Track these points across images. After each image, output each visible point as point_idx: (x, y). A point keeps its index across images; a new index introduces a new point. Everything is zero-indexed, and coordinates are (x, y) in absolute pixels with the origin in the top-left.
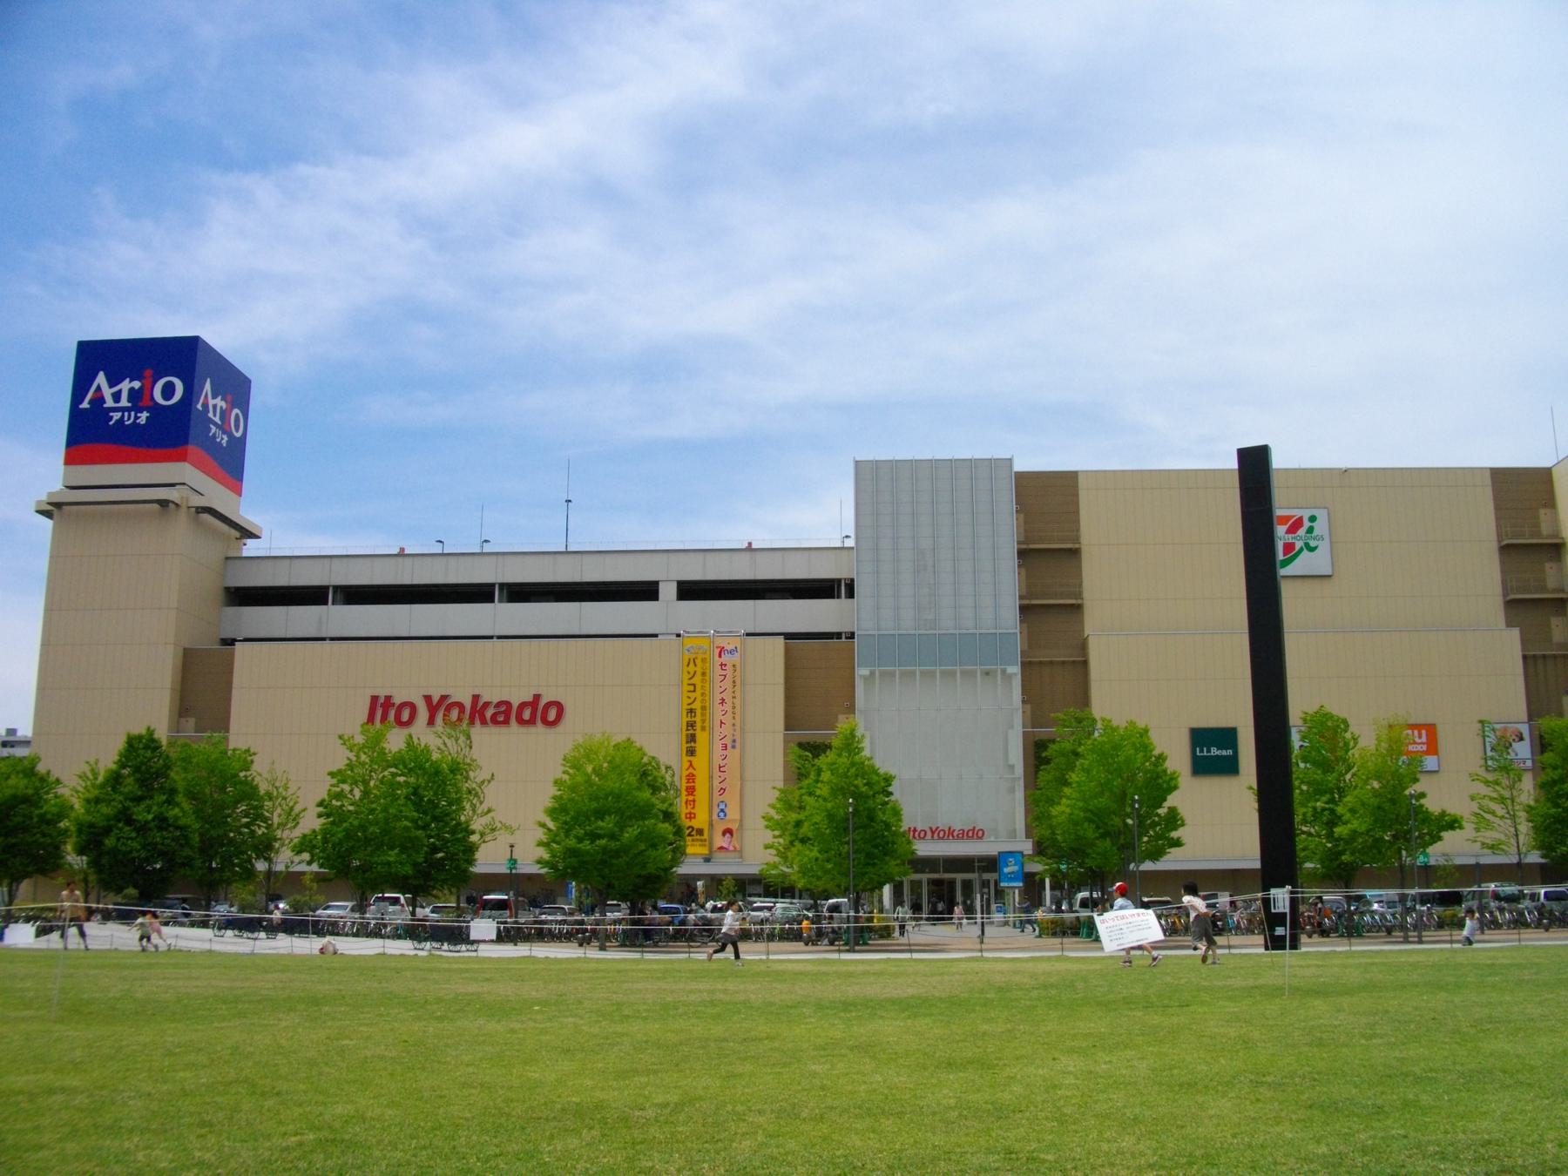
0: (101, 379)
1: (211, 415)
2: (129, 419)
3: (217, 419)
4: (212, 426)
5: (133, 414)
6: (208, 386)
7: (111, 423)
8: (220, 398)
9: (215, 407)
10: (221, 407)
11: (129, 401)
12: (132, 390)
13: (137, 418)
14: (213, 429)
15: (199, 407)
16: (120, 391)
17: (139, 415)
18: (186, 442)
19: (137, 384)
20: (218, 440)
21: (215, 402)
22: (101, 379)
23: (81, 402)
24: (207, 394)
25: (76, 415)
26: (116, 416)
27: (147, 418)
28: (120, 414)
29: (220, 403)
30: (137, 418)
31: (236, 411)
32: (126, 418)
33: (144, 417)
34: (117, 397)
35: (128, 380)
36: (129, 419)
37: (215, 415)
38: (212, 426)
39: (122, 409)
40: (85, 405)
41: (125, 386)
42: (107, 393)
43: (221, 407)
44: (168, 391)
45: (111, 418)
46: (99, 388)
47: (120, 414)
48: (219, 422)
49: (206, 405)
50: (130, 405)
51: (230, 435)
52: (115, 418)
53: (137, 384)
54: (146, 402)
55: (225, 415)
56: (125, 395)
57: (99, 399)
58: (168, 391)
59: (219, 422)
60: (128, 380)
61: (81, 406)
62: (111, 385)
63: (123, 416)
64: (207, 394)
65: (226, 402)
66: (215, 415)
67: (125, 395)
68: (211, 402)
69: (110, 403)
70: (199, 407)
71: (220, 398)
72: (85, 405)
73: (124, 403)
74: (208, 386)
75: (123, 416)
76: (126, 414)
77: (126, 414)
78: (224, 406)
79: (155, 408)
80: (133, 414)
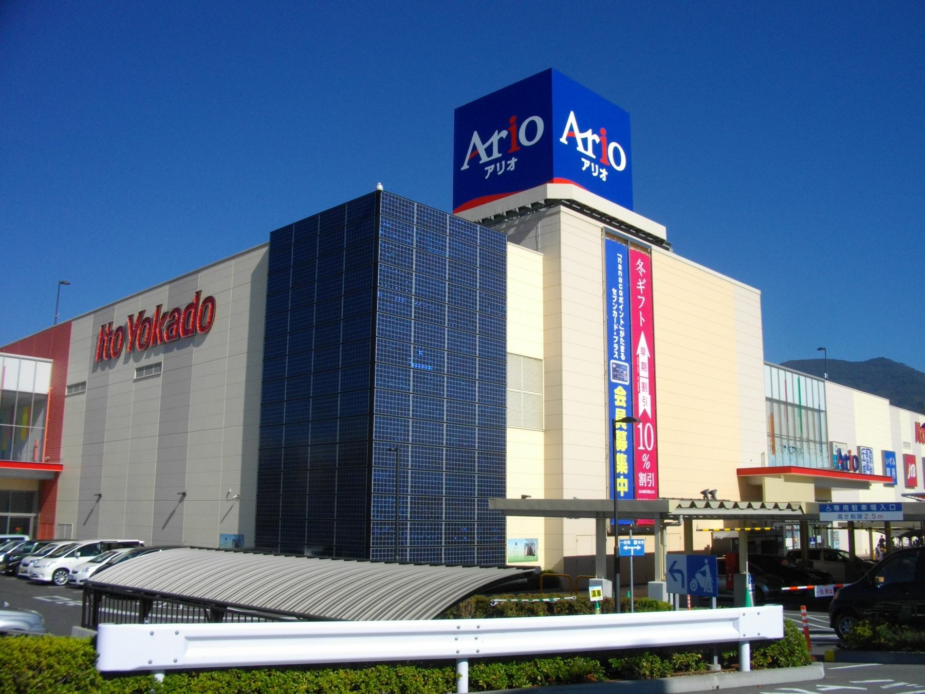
0: (476, 138)
1: (580, 148)
2: (501, 169)
3: (590, 153)
4: (583, 160)
5: (503, 163)
6: (572, 119)
7: (487, 177)
8: (590, 131)
9: (585, 141)
10: (594, 141)
11: (499, 152)
12: (501, 141)
13: (507, 166)
14: (587, 163)
15: (563, 140)
16: (492, 144)
17: (509, 162)
18: (553, 178)
19: (504, 134)
20: (595, 174)
21: (584, 135)
22: (476, 138)
23: (462, 165)
24: (571, 126)
25: (459, 176)
26: (490, 169)
27: (516, 163)
28: (493, 166)
29: (590, 135)
30: (507, 166)
31: (613, 145)
32: (498, 170)
34: (489, 151)
35: (497, 132)
36: (501, 169)
37: (586, 148)
38: (583, 160)
39: (494, 162)
40: (465, 166)
41: (495, 139)
42: (481, 149)
43: (594, 141)
46: (474, 146)
47: (493, 166)
48: (594, 157)
49: (572, 139)
50: (500, 155)
51: (610, 169)
52: (490, 171)
53: (504, 134)
55: (599, 149)
57: (476, 157)
59: (594, 157)
61: (462, 169)
63: (496, 167)
64: (571, 126)
65: (599, 135)
66: (586, 148)
68: (579, 136)
69: (484, 158)
70: (563, 140)
71: (590, 131)
73: (496, 154)
74: (572, 119)
75: (496, 167)
76: (498, 165)
77: (498, 165)
78: (598, 140)
80: (503, 163)
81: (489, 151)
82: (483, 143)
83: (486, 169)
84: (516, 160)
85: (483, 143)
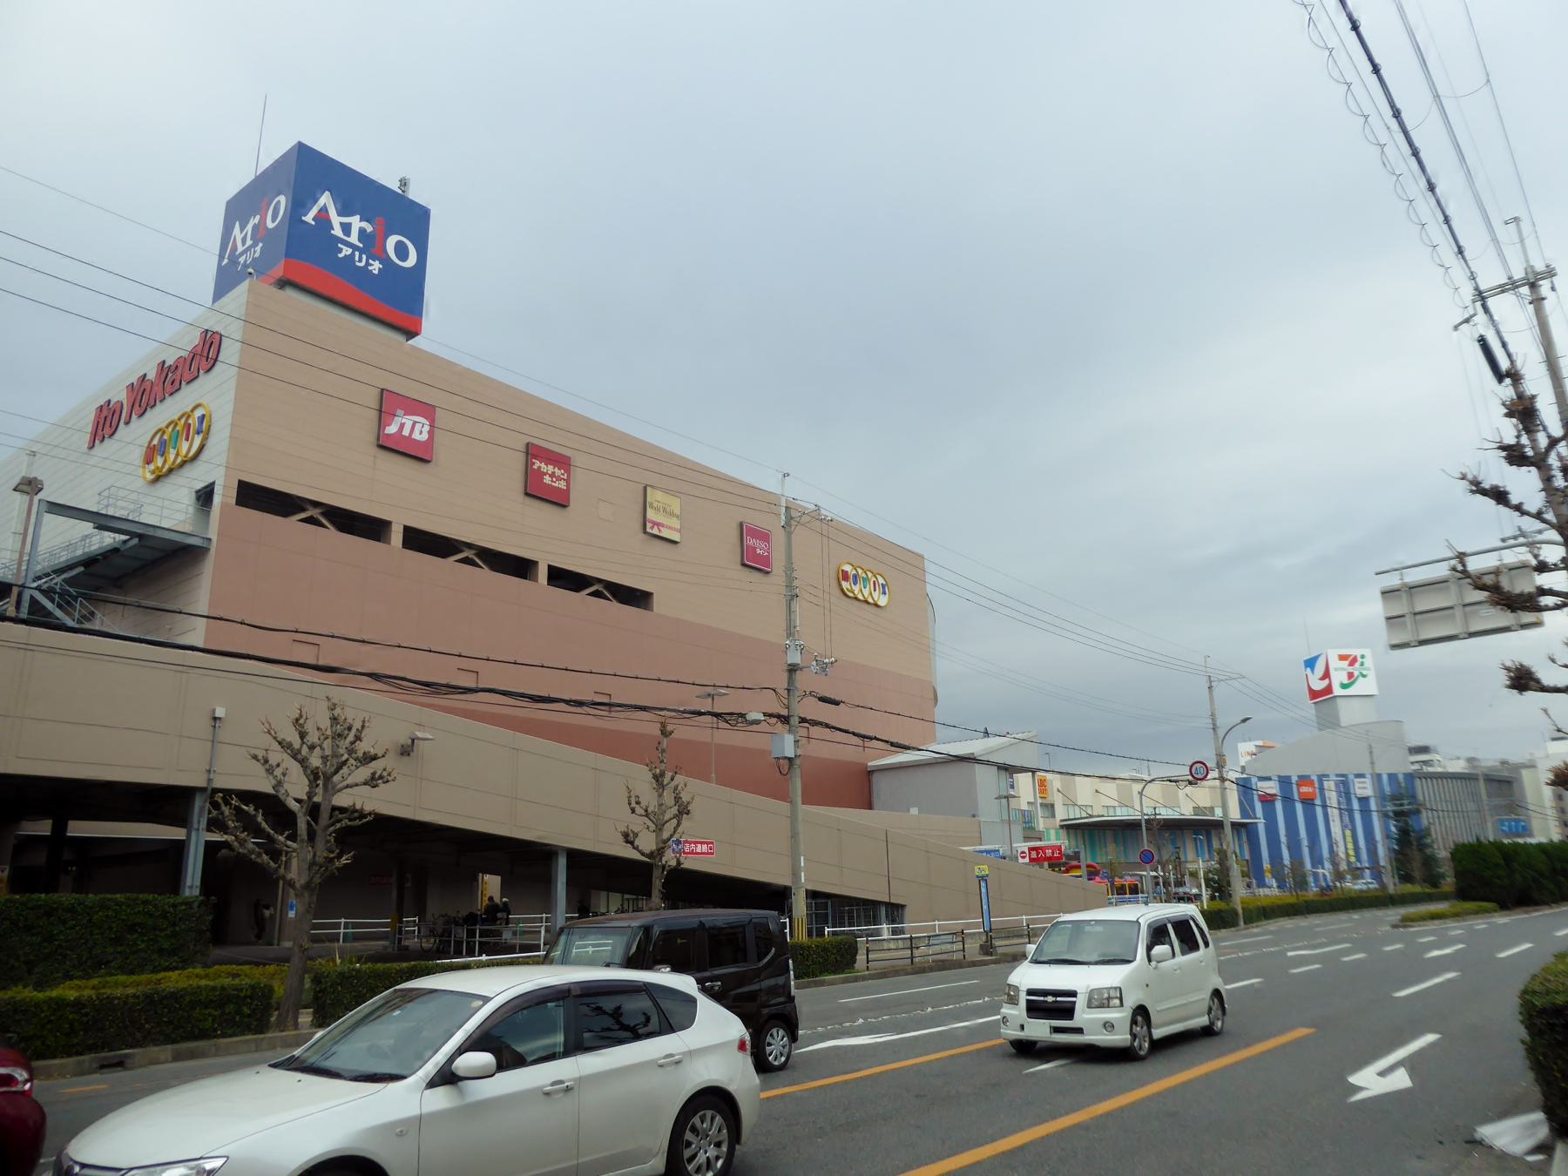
0: (325, 199)
2: (360, 261)
5: (364, 257)
7: (341, 255)
11: (359, 240)
13: (368, 264)
17: (371, 261)
19: (369, 228)
22: (325, 199)
26: (347, 251)
28: (350, 251)
32: (357, 259)
33: (376, 267)
34: (346, 228)
35: (358, 217)
40: (309, 218)
42: (336, 220)
44: (401, 251)
45: (340, 250)
47: (350, 251)
53: (369, 228)
57: (323, 216)
58: (401, 251)
60: (358, 217)
63: (353, 254)
72: (309, 218)
75: (353, 254)
76: (357, 253)
77: (357, 253)
79: (385, 259)
80: (364, 257)
81: (346, 228)
83: (340, 245)
84: (381, 266)
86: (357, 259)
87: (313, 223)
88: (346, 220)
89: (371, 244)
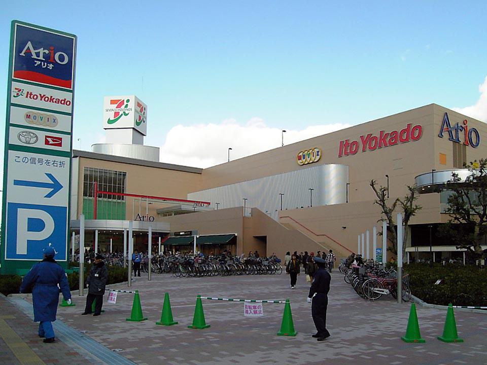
0: (29, 44)
2: (44, 65)
5: (46, 64)
13: (47, 66)
19: (47, 52)
22: (29, 44)
32: (43, 65)
34: (38, 54)
35: (42, 49)
36: (44, 65)
40: (22, 54)
42: (33, 52)
44: (62, 58)
50: (44, 59)
53: (47, 52)
54: (51, 60)
56: (41, 55)
57: (28, 52)
58: (62, 58)
60: (42, 49)
62: (35, 49)
63: (41, 64)
67: (41, 55)
69: (34, 56)
73: (41, 58)
76: (43, 63)
77: (43, 63)
79: (55, 63)
80: (46, 64)
81: (38, 54)
82: (39, 52)
85: (39, 52)
86: (43, 65)
87: (24, 55)
88: (37, 51)
89: (48, 58)
